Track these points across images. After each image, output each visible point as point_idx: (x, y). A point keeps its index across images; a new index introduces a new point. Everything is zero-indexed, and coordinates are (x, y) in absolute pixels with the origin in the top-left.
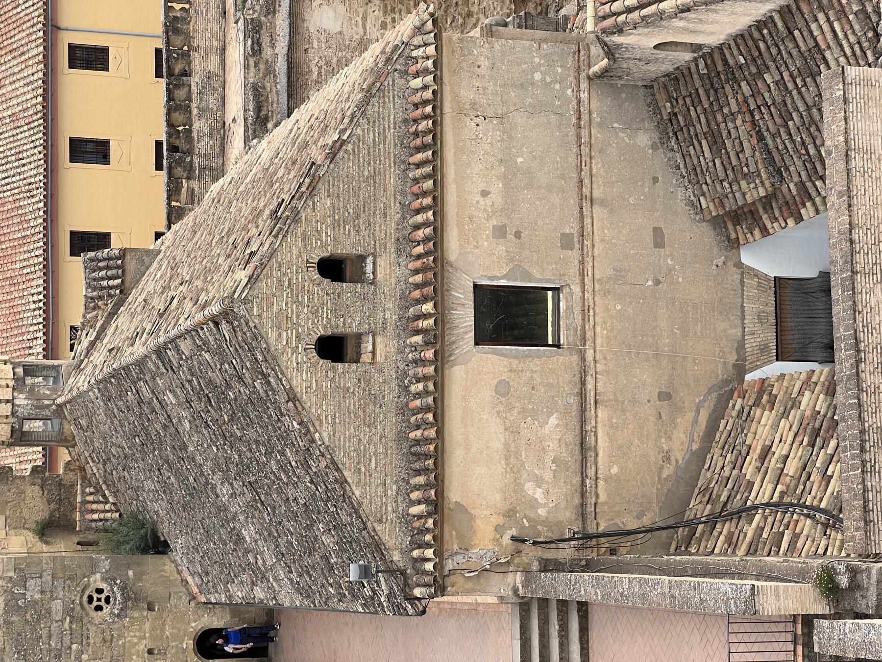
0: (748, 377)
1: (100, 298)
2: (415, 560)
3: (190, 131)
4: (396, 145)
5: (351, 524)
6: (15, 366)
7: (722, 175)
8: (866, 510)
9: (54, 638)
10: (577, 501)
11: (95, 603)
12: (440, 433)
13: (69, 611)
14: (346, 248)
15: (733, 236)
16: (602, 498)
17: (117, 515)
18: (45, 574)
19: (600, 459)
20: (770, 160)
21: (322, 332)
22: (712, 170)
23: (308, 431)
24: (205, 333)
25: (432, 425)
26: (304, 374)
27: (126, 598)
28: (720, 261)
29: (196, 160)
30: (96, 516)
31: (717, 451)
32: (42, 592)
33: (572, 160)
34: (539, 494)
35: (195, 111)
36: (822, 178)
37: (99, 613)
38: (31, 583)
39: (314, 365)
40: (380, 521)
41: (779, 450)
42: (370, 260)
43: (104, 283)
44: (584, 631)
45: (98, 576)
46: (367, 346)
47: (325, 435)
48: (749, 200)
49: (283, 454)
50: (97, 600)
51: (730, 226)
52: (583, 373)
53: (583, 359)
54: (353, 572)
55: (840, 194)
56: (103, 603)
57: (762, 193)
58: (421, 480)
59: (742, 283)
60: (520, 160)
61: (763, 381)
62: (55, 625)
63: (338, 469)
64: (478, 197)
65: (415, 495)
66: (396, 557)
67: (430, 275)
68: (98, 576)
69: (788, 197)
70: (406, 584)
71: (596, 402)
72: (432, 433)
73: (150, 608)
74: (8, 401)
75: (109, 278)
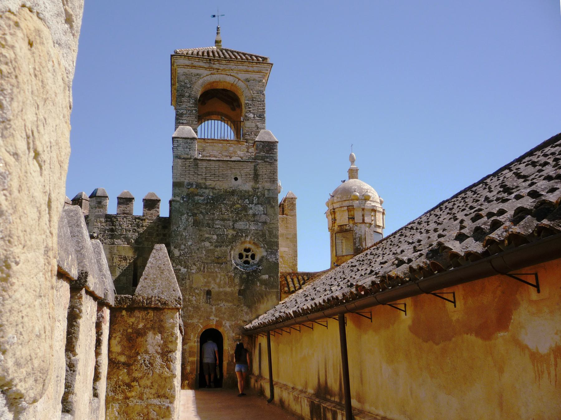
9: (222, 223)
11: (245, 254)
18: (267, 217)
30: (289, 280)
32: (254, 215)
37: (237, 256)
45: (265, 254)
56: (244, 259)
68: (265, 254)
73: (240, 292)
74: (363, 220)
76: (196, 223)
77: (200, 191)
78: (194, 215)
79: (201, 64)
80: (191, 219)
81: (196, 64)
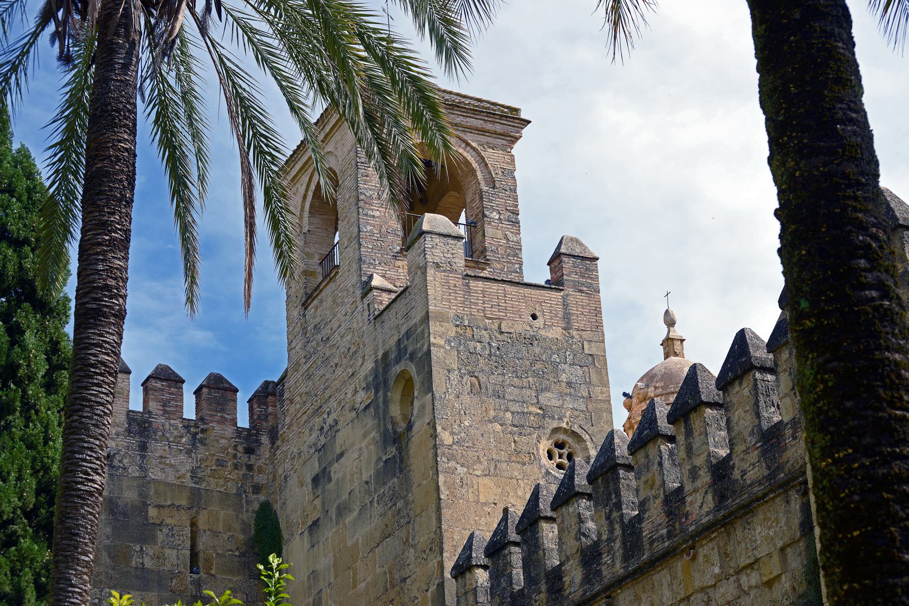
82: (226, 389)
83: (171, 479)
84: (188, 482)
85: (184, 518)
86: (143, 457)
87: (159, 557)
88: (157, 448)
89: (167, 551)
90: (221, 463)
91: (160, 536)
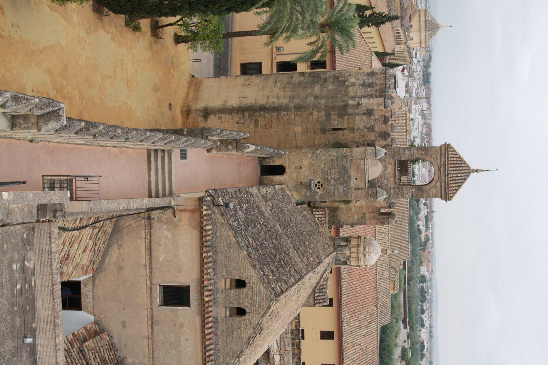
0: (91, 275)
1: (322, 289)
2: (209, 210)
3: (292, 347)
4: (219, 356)
5: (233, 222)
6: (350, 265)
7: (101, 349)
8: (50, 238)
10: (152, 230)
11: (320, 184)
12: (202, 255)
13: (329, 181)
14: (237, 319)
15: (97, 326)
16: (143, 232)
17: (314, 213)
19: (144, 245)
20: (84, 355)
21: (245, 290)
22: (105, 350)
23: (248, 255)
24: (285, 286)
25: (205, 258)
26: (250, 274)
27: (310, 186)
28: (102, 316)
29: (290, 337)
30: (321, 213)
31: (102, 249)
32: (338, 188)
33: (156, 353)
34: (166, 233)
35: (291, 354)
36: (65, 350)
38: (342, 191)
39: (247, 278)
40: (222, 223)
41: (80, 251)
42: (228, 315)
43: (321, 294)
44: (150, 186)
45: (319, 194)
46: (228, 285)
47: (242, 253)
48: (91, 340)
49: (257, 245)
50: (320, 185)
51: (98, 330)
52: (150, 276)
53: (151, 281)
54: (231, 205)
55: (59, 349)
56: (318, 184)
57: (87, 343)
58: (208, 238)
59: (93, 309)
60: (174, 352)
61: (86, 274)
62: (333, 177)
63: (237, 241)
64: (189, 338)
65: (210, 232)
66: (216, 211)
67: (206, 311)
68: (319, 194)
69: (77, 342)
70: (213, 201)
71: (146, 266)
72: (204, 255)
73: (301, 183)
75: (319, 296)
76: (332, 160)
77: (349, 162)
78: (337, 159)
79: (443, 160)
80: (335, 158)
81: (443, 157)
82: (385, 137)
83: (356, 122)
84: (356, 127)
85: (346, 126)
86: (361, 114)
87: (334, 120)
88: (364, 118)
89: (336, 122)
90: (363, 136)
91: (340, 120)
